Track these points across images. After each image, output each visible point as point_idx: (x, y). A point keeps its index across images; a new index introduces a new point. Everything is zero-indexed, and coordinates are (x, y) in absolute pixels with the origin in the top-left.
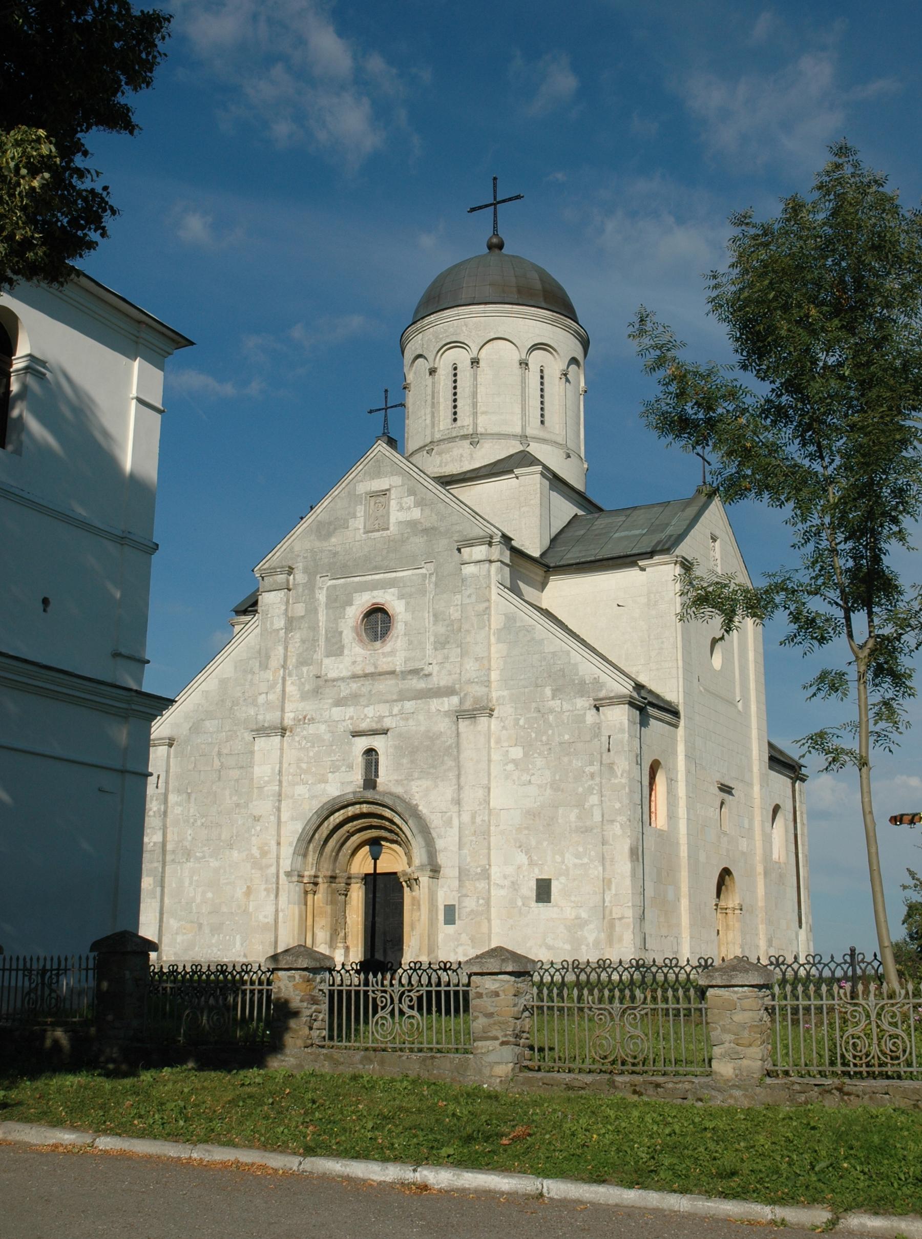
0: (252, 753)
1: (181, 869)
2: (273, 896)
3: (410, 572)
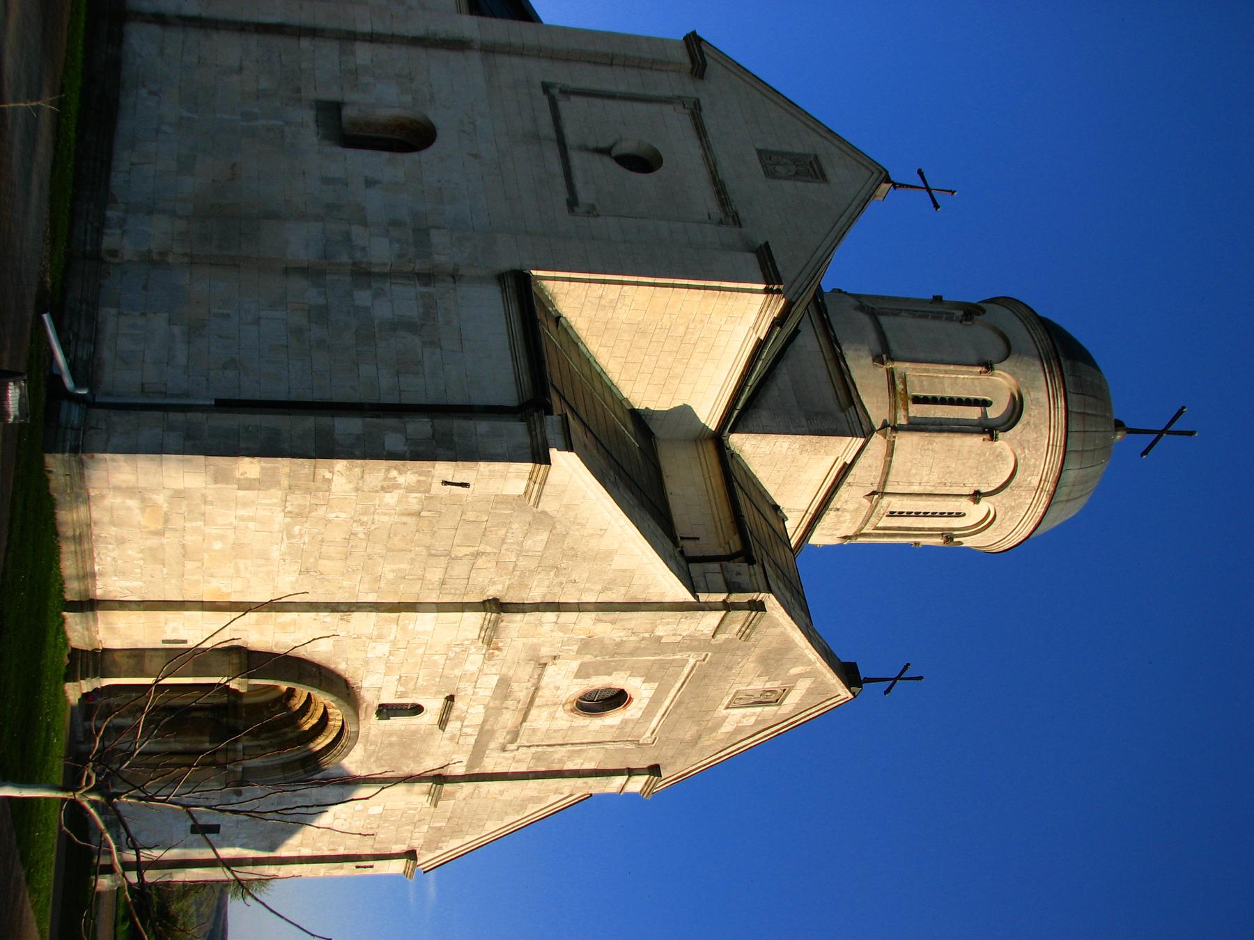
1: (274, 505)
3: (653, 725)
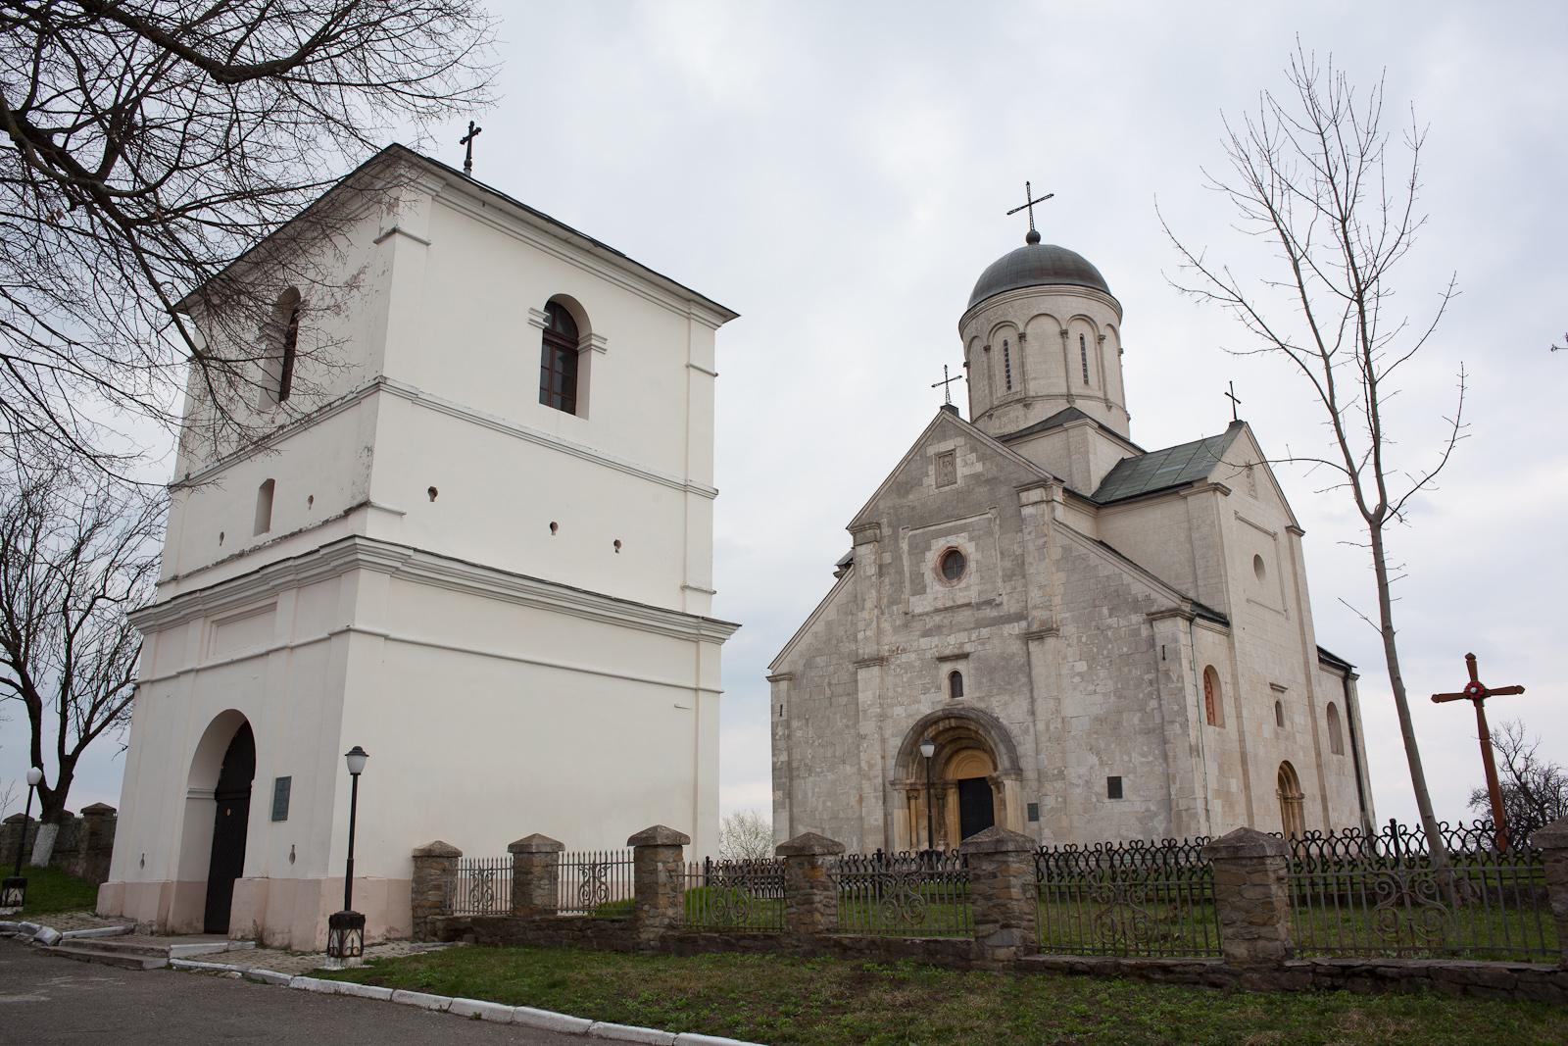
0: (856, 681)
2: (881, 802)
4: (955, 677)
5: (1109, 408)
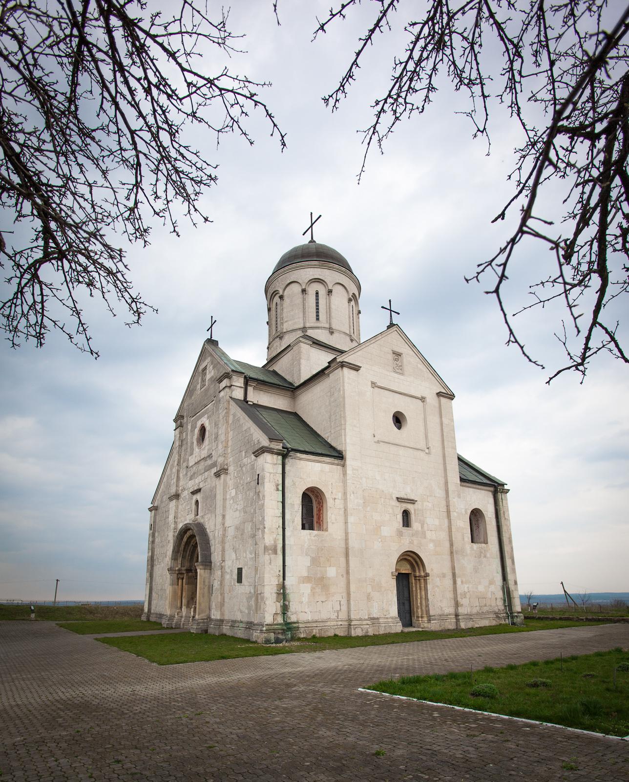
4: (197, 502)
5: (332, 333)
